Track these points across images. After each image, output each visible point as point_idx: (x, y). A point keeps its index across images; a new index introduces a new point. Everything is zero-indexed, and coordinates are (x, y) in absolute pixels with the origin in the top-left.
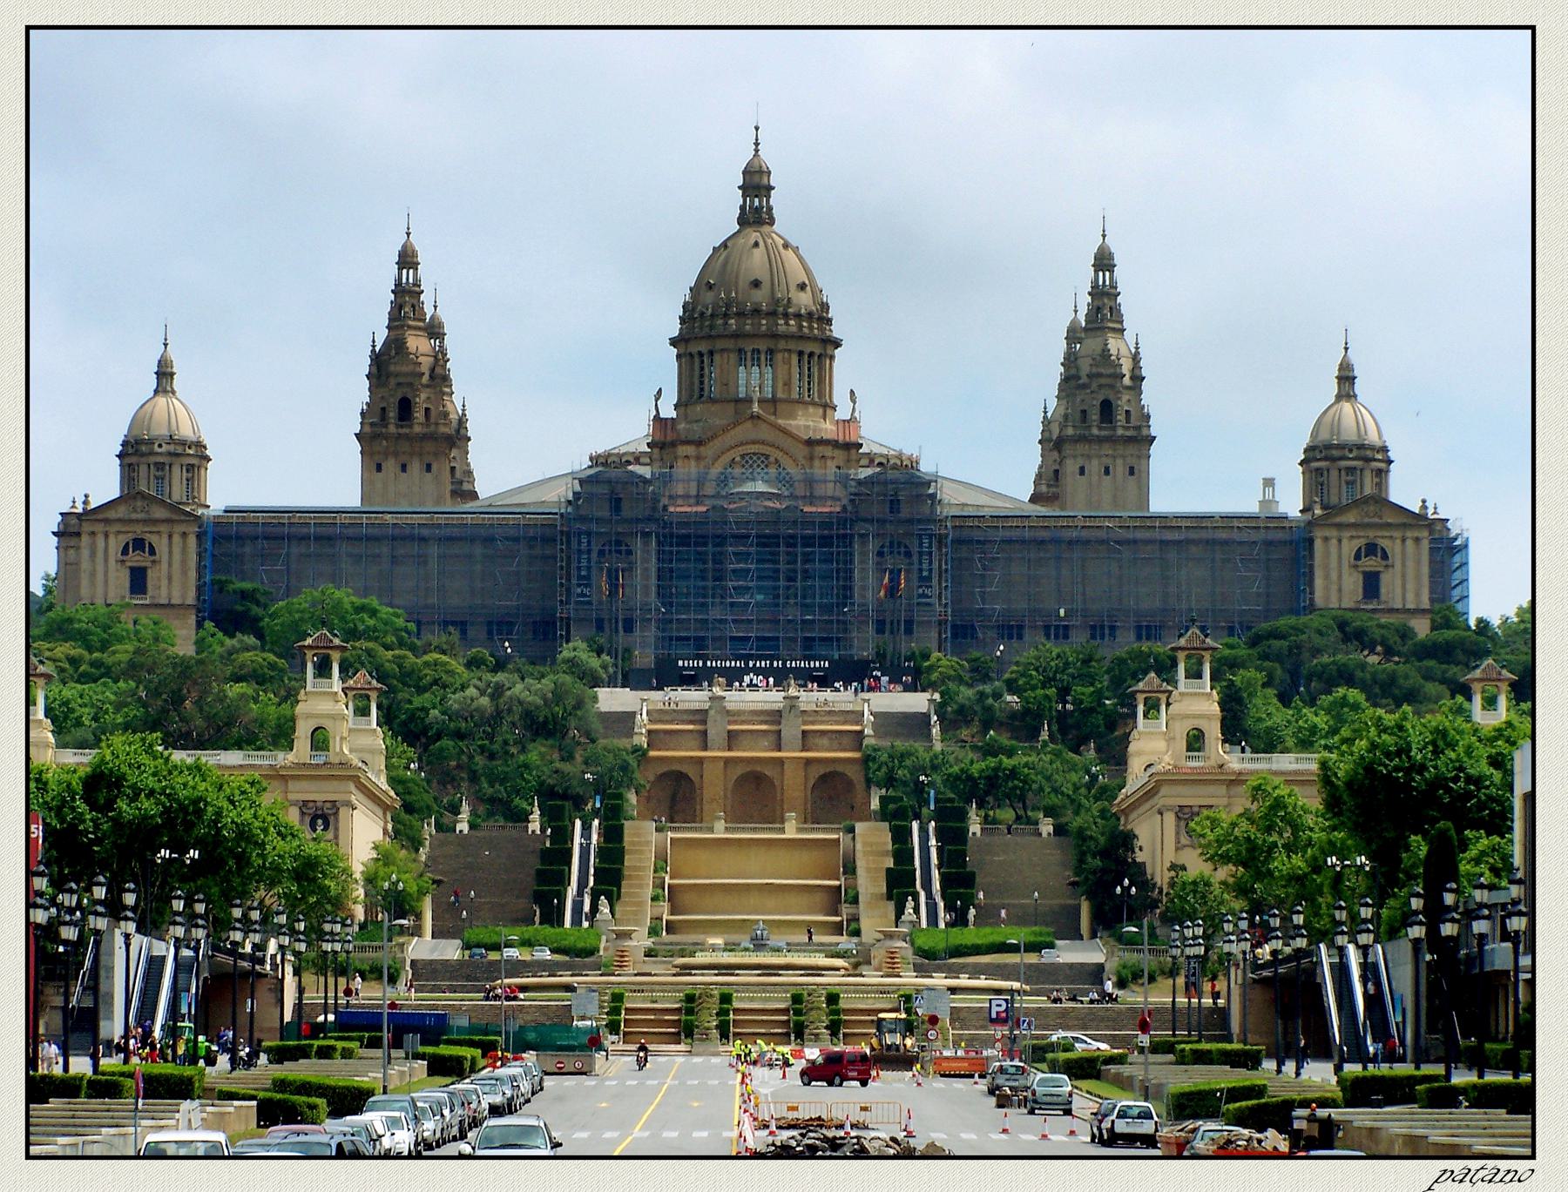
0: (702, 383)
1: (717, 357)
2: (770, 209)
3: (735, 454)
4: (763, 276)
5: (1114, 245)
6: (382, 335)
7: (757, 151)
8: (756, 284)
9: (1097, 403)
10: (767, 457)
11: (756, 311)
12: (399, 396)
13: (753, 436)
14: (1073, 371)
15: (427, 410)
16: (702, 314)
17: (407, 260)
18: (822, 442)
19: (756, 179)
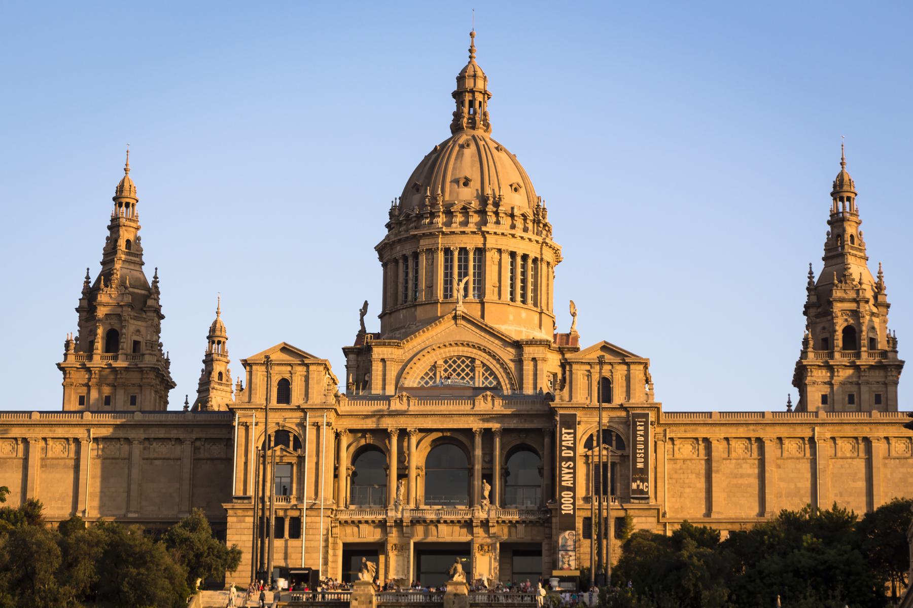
0: (406, 289)
2: (485, 114)
3: (438, 357)
5: (851, 173)
7: (470, 57)
9: (839, 329)
10: (473, 360)
13: (457, 338)
15: (136, 344)
18: (532, 343)
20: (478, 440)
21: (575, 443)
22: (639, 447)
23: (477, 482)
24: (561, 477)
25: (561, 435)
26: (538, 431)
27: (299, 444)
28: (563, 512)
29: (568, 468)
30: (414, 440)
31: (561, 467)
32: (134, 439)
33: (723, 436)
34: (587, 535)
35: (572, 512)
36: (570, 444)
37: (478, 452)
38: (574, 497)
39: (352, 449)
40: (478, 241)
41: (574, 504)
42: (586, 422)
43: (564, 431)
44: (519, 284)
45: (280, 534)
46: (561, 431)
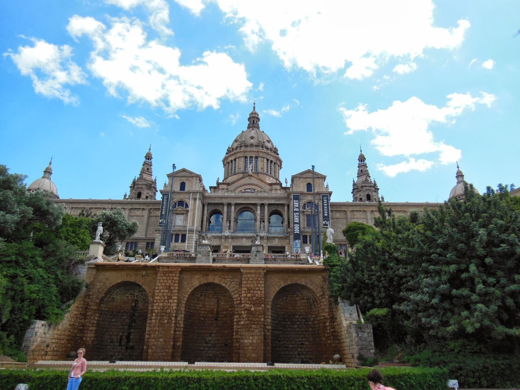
1: (237, 160)
4: (255, 136)
5: (363, 153)
6: (138, 176)
7: (254, 110)
8: (252, 138)
10: (254, 190)
11: (252, 145)
12: (138, 191)
14: (356, 187)
16: (233, 149)
17: (149, 157)
19: (254, 115)
23: (258, 223)
26: (283, 205)
27: (187, 206)
30: (233, 207)
32: (127, 209)
33: (351, 210)
34: (305, 242)
37: (259, 212)
38: (299, 227)
39: (209, 211)
40: (257, 154)
41: (299, 229)
42: (303, 199)
44: (269, 168)
45: (177, 241)
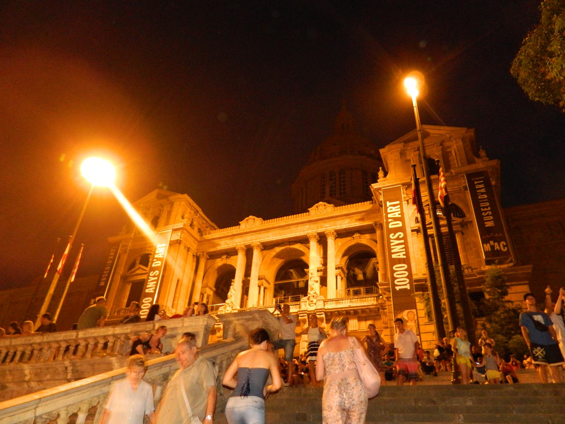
20: (313, 244)
21: (402, 214)
22: (482, 205)
24: (390, 249)
25: (386, 208)
28: (397, 288)
29: (398, 239)
31: (389, 239)
35: (408, 287)
36: (397, 215)
41: (410, 276)
43: (388, 204)
46: (386, 204)
